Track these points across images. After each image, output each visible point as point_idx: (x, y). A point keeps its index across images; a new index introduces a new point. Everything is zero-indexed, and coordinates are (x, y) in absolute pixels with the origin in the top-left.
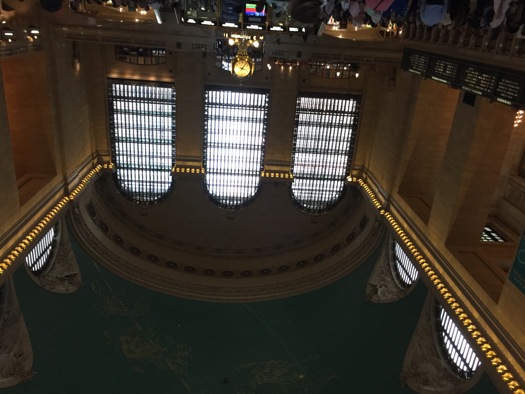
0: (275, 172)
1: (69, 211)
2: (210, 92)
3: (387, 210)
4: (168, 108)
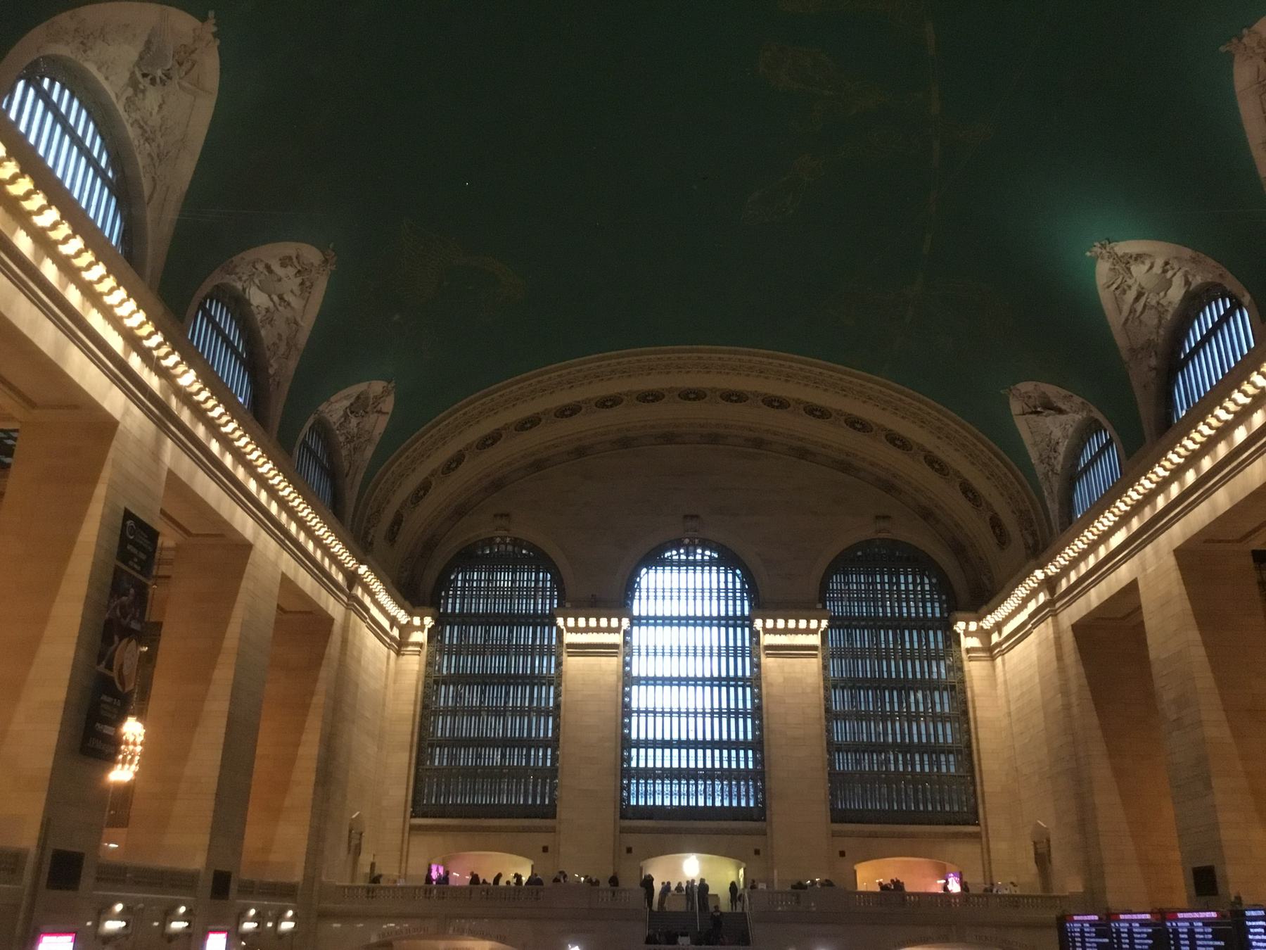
0: (598, 630)
3: (353, 578)
4: (844, 763)
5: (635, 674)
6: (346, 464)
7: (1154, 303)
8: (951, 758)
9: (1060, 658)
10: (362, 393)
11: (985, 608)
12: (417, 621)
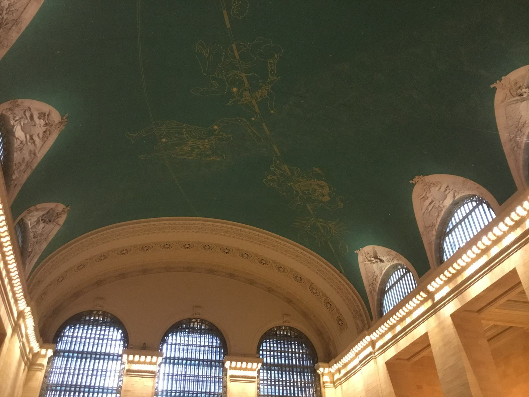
0: (144, 363)
3: (21, 314)
6: (30, 250)
7: (437, 206)
10: (52, 209)
11: (333, 361)
12: (43, 352)
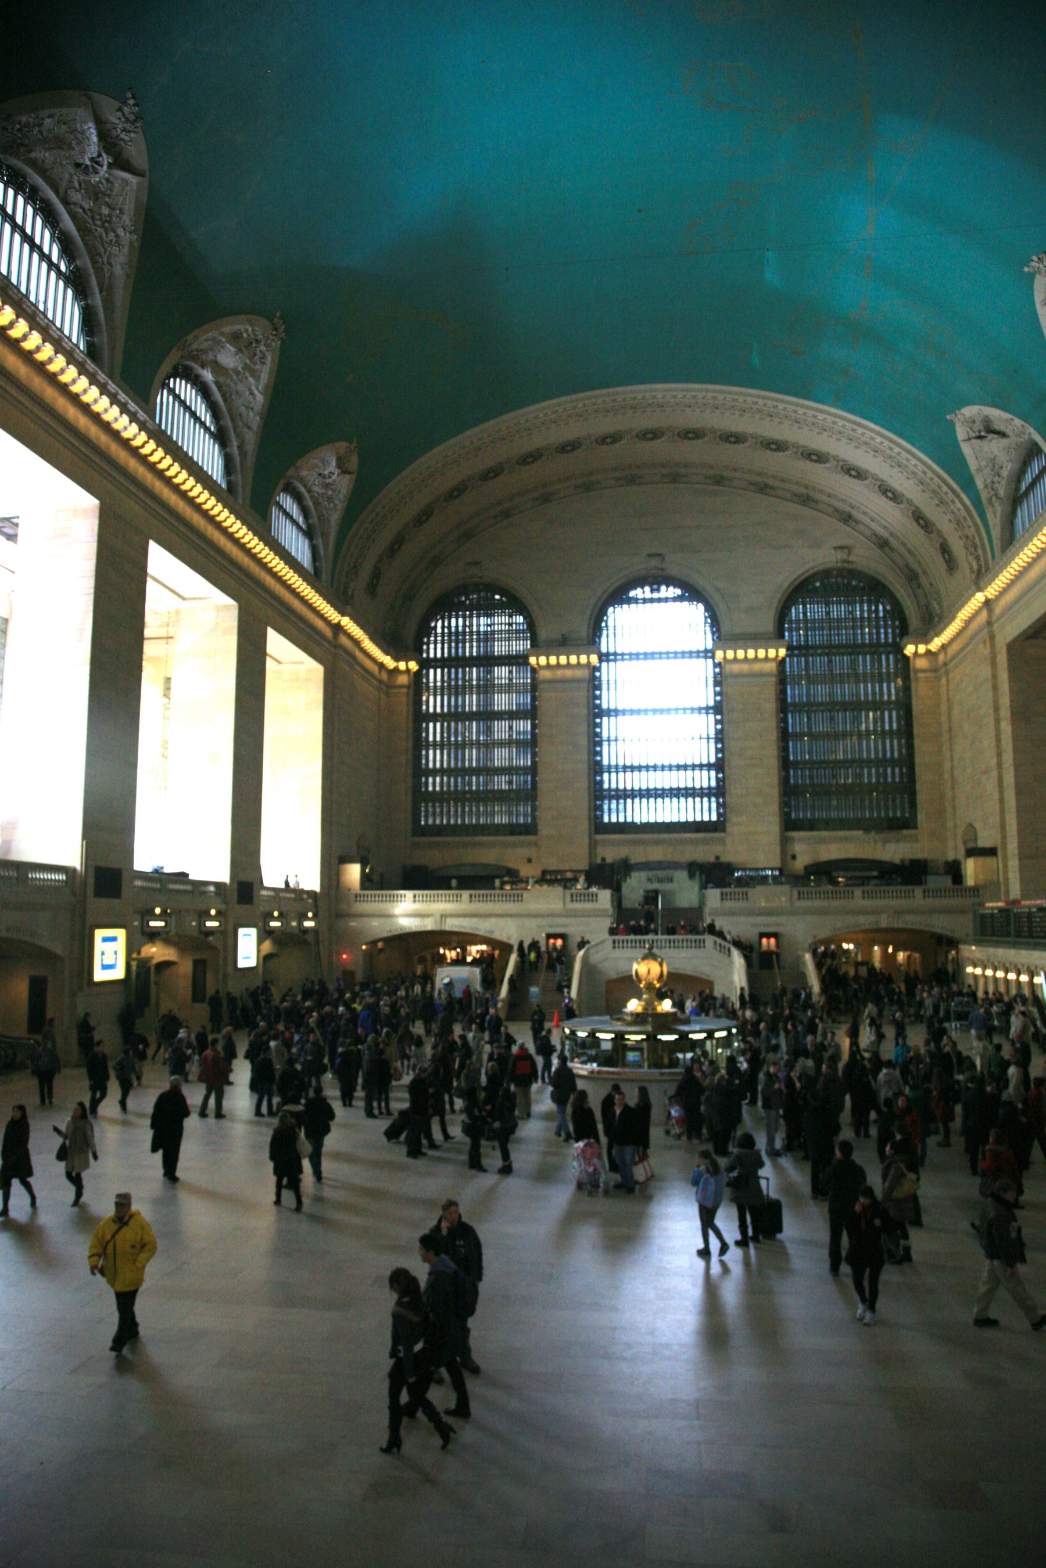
1: (987, 569)
2: (714, 818)
3: (338, 628)
5: (605, 706)
8: (897, 770)
9: (994, 676)
11: (932, 633)
12: (402, 665)
